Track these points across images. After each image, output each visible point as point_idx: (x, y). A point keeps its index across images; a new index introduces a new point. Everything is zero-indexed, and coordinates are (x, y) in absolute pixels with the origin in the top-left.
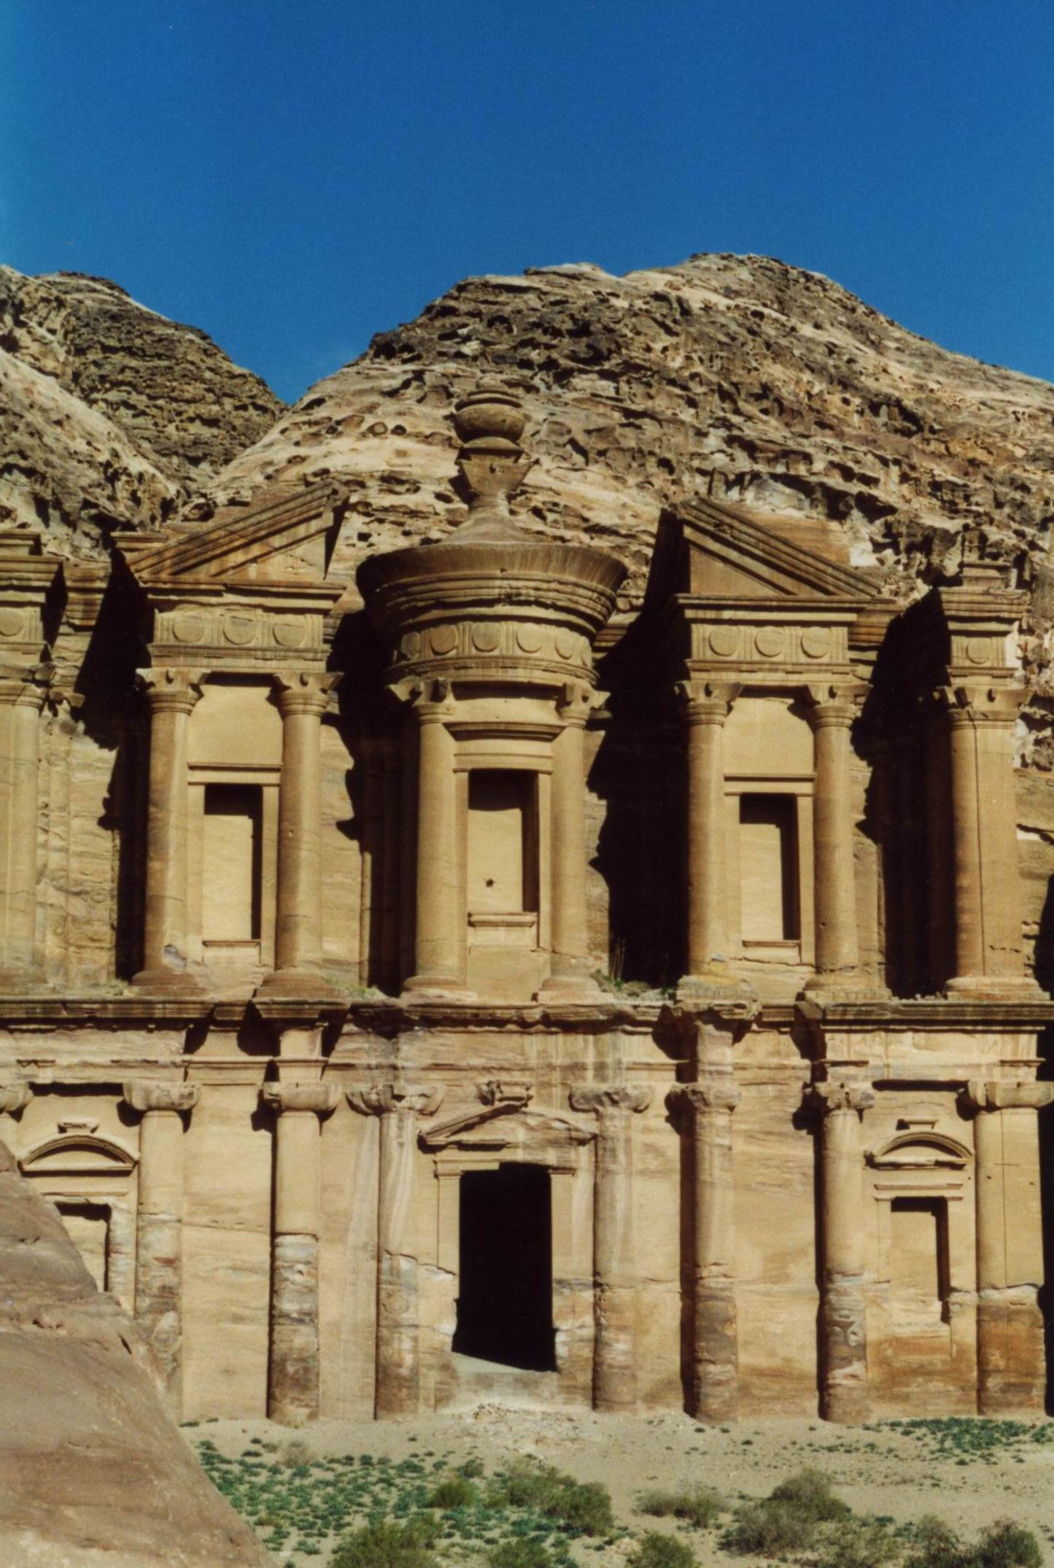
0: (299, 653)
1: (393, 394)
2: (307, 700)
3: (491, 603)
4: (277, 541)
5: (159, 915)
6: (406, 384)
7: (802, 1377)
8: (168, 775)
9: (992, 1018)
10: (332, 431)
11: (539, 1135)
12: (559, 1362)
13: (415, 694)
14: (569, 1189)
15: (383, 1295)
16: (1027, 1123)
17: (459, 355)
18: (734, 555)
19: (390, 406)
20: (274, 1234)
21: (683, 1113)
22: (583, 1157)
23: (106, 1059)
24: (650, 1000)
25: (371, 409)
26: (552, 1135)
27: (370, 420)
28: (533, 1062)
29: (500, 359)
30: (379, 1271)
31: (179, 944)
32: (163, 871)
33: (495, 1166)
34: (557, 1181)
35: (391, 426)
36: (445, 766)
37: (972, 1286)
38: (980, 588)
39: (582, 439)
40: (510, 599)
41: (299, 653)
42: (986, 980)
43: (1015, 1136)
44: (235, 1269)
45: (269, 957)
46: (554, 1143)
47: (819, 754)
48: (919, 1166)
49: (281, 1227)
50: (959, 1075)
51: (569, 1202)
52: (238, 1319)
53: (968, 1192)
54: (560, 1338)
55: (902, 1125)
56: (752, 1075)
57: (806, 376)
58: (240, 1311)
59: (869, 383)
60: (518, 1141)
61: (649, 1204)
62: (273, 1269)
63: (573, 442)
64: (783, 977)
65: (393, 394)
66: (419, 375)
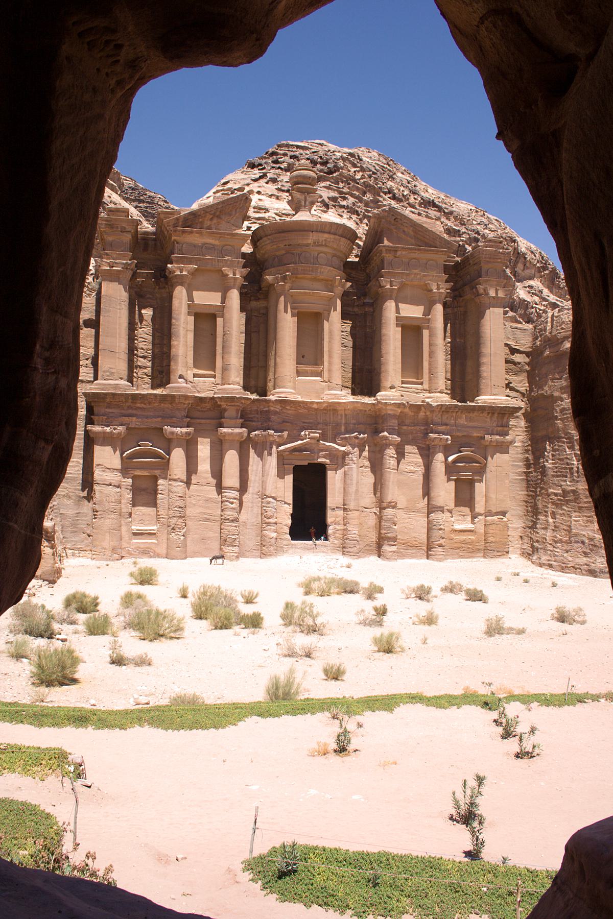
1: (256, 180)
2: (235, 279)
5: (176, 362)
6: (261, 177)
8: (180, 307)
17: (279, 168)
19: (256, 184)
25: (248, 185)
31: (184, 374)
39: (327, 200)
45: (218, 380)
51: (334, 479)
57: (402, 188)
59: (422, 194)
63: (323, 200)
64: (415, 395)
65: (256, 180)
66: (264, 176)
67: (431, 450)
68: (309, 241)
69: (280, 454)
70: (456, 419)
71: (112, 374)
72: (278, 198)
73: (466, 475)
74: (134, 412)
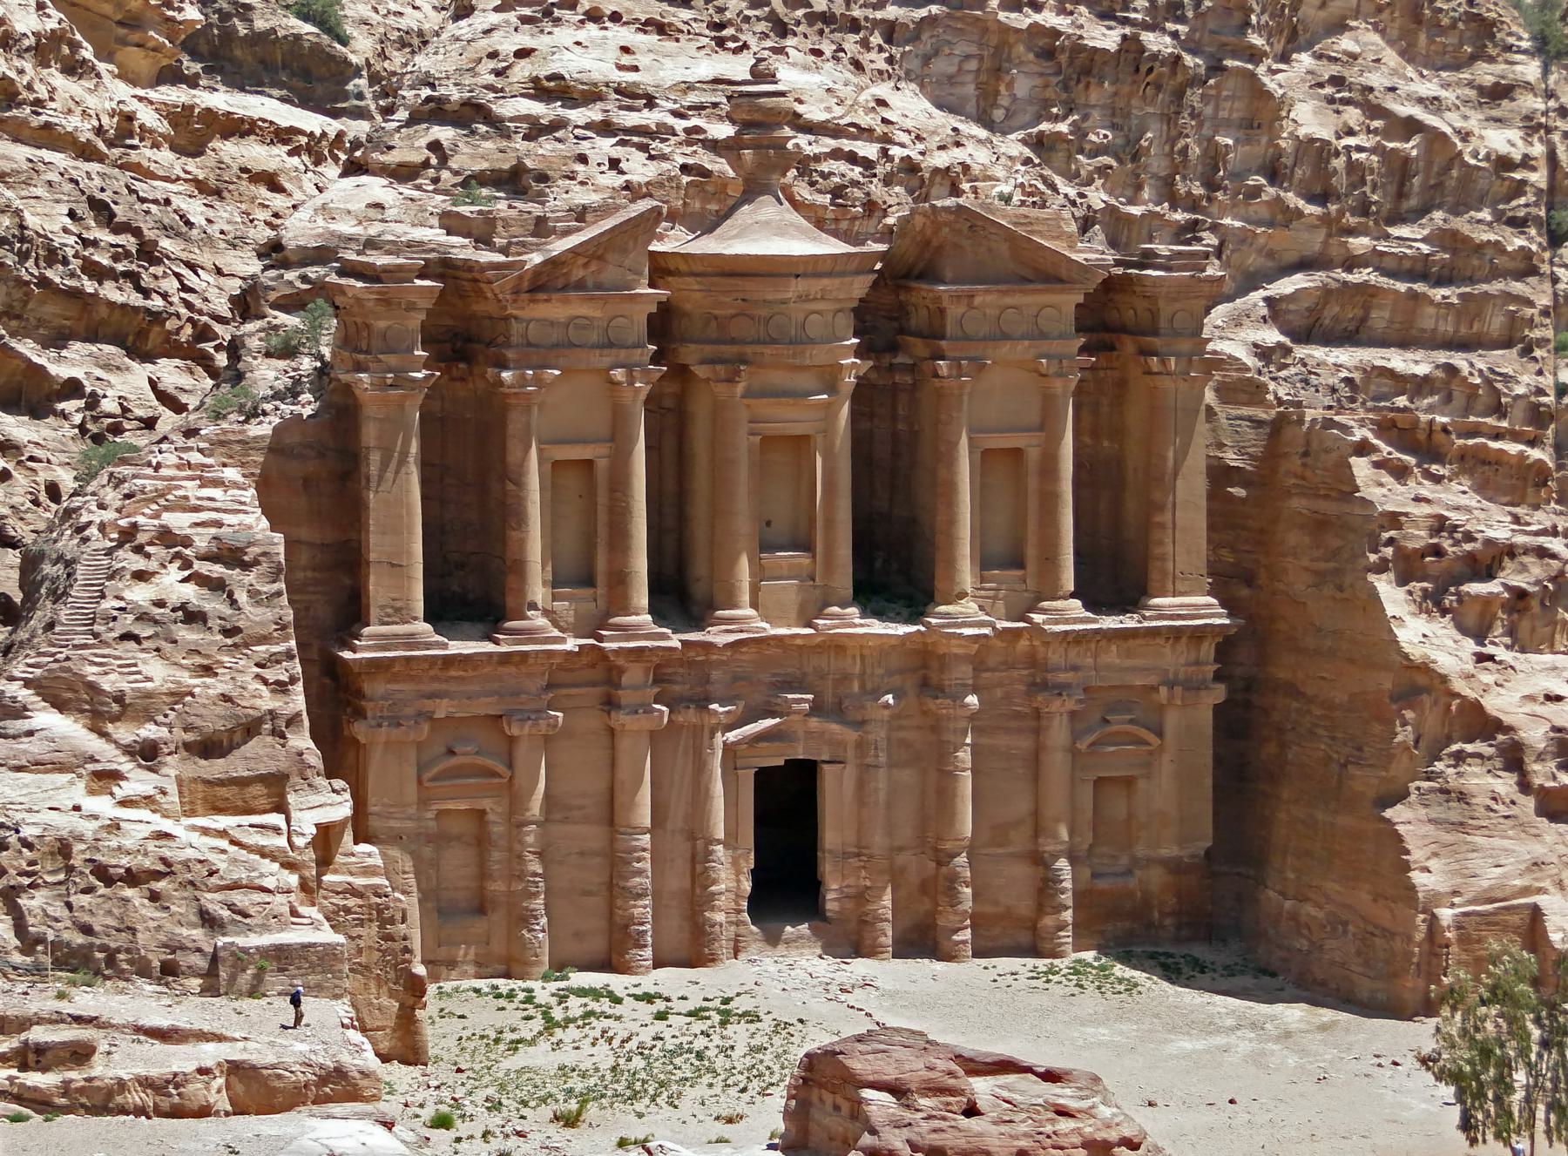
67: (1044, 722)
68: (790, 295)
70: (1096, 656)
71: (397, 610)
72: (661, 29)
74: (444, 686)
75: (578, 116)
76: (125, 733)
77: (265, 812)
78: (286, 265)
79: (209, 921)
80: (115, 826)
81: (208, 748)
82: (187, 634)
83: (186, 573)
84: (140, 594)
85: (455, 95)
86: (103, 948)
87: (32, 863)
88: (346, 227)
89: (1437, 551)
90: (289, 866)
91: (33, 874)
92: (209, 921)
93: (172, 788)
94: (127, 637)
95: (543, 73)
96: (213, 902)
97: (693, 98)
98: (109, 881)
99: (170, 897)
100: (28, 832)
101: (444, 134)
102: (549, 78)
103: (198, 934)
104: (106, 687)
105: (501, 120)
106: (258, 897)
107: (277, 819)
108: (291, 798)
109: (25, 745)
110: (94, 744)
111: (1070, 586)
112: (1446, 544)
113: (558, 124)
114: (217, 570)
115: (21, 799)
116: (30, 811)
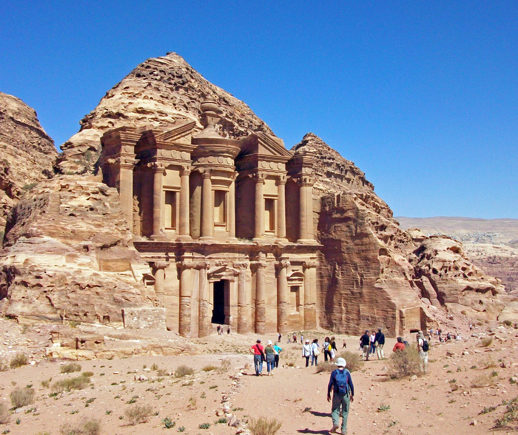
0: (186, 161)
3: (223, 152)
4: (183, 134)
5: (158, 221)
7: (274, 324)
9: (310, 249)
10: (134, 96)
11: (228, 273)
12: (230, 323)
13: (205, 172)
14: (233, 285)
15: (201, 310)
16: (314, 270)
17: (156, 79)
18: (266, 146)
20: (181, 296)
21: (255, 269)
22: (236, 279)
23: (151, 256)
24: (246, 243)
26: (231, 273)
27: (143, 95)
28: (226, 257)
29: (164, 82)
30: (200, 304)
32: (160, 211)
33: (219, 280)
34: (231, 284)
35: (150, 97)
36: (210, 189)
37: (303, 304)
38: (309, 157)
40: (227, 152)
41: (186, 161)
42: (308, 240)
43: (312, 273)
44: (172, 305)
45: (178, 232)
46: (230, 275)
47: (279, 191)
48: (295, 280)
49: (182, 295)
50: (303, 260)
51: (233, 288)
52: (173, 316)
53: (303, 285)
54: (231, 318)
55: (293, 271)
56: (267, 261)
58: (173, 314)
60: (225, 275)
61: (248, 287)
62: (180, 305)
69: (209, 276)
72: (163, 102)
73: (296, 283)
75: (149, 116)
76: (75, 243)
77: (123, 271)
78: (73, 147)
79: (117, 302)
80: (79, 272)
81: (104, 247)
82: (90, 214)
83: (88, 197)
84: (74, 203)
85: (115, 111)
86: (83, 311)
87: (52, 283)
88: (89, 138)
89: (377, 223)
90: (136, 286)
91: (53, 286)
92: (117, 302)
93: (95, 261)
94: (72, 215)
95: (137, 107)
96: (118, 296)
97: (175, 116)
98: (82, 288)
99: (103, 295)
100: (48, 273)
101: (112, 120)
102: (139, 108)
103: (114, 307)
104: (68, 228)
105: (128, 117)
106: (132, 296)
107: (129, 272)
108: (133, 266)
109: (42, 245)
110: (67, 247)
111: (285, 235)
112: (379, 222)
113: (142, 118)
114: (99, 196)
115: (45, 262)
116: (48, 266)
